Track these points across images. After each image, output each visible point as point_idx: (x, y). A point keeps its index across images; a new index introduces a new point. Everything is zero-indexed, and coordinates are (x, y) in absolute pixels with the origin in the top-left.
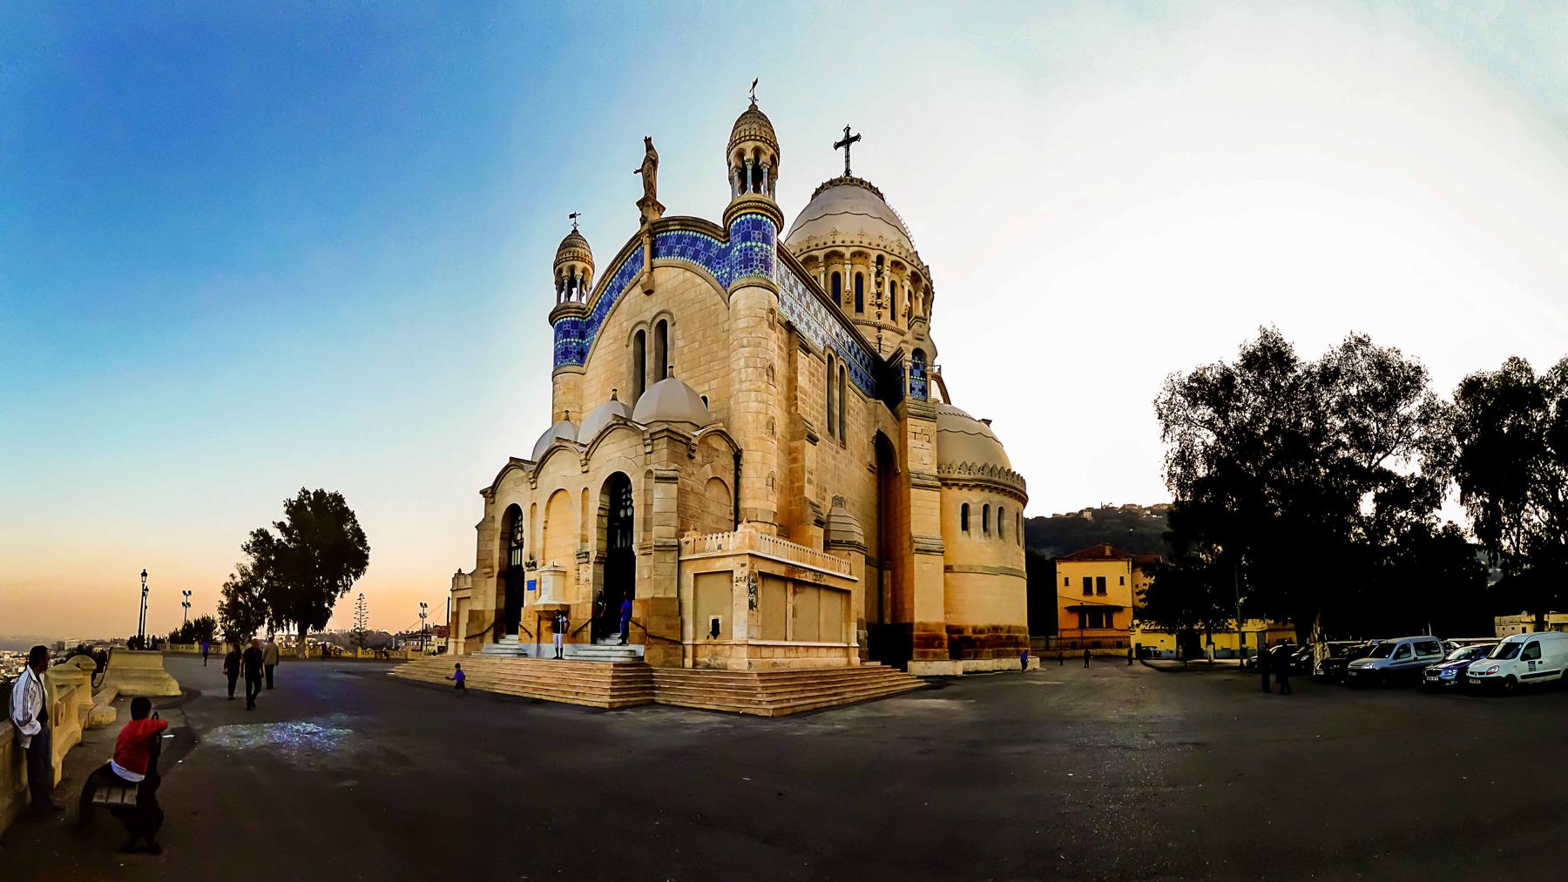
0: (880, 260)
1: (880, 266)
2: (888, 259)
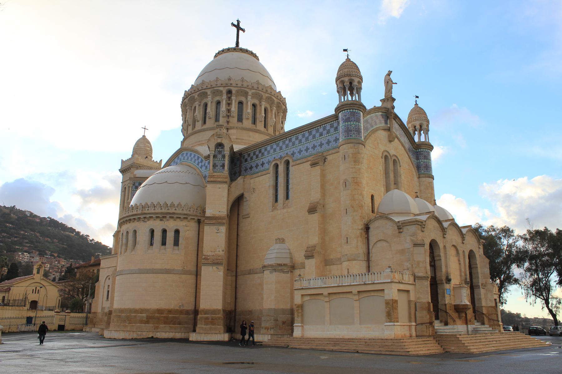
0: (229, 92)
1: (229, 95)
2: (234, 90)
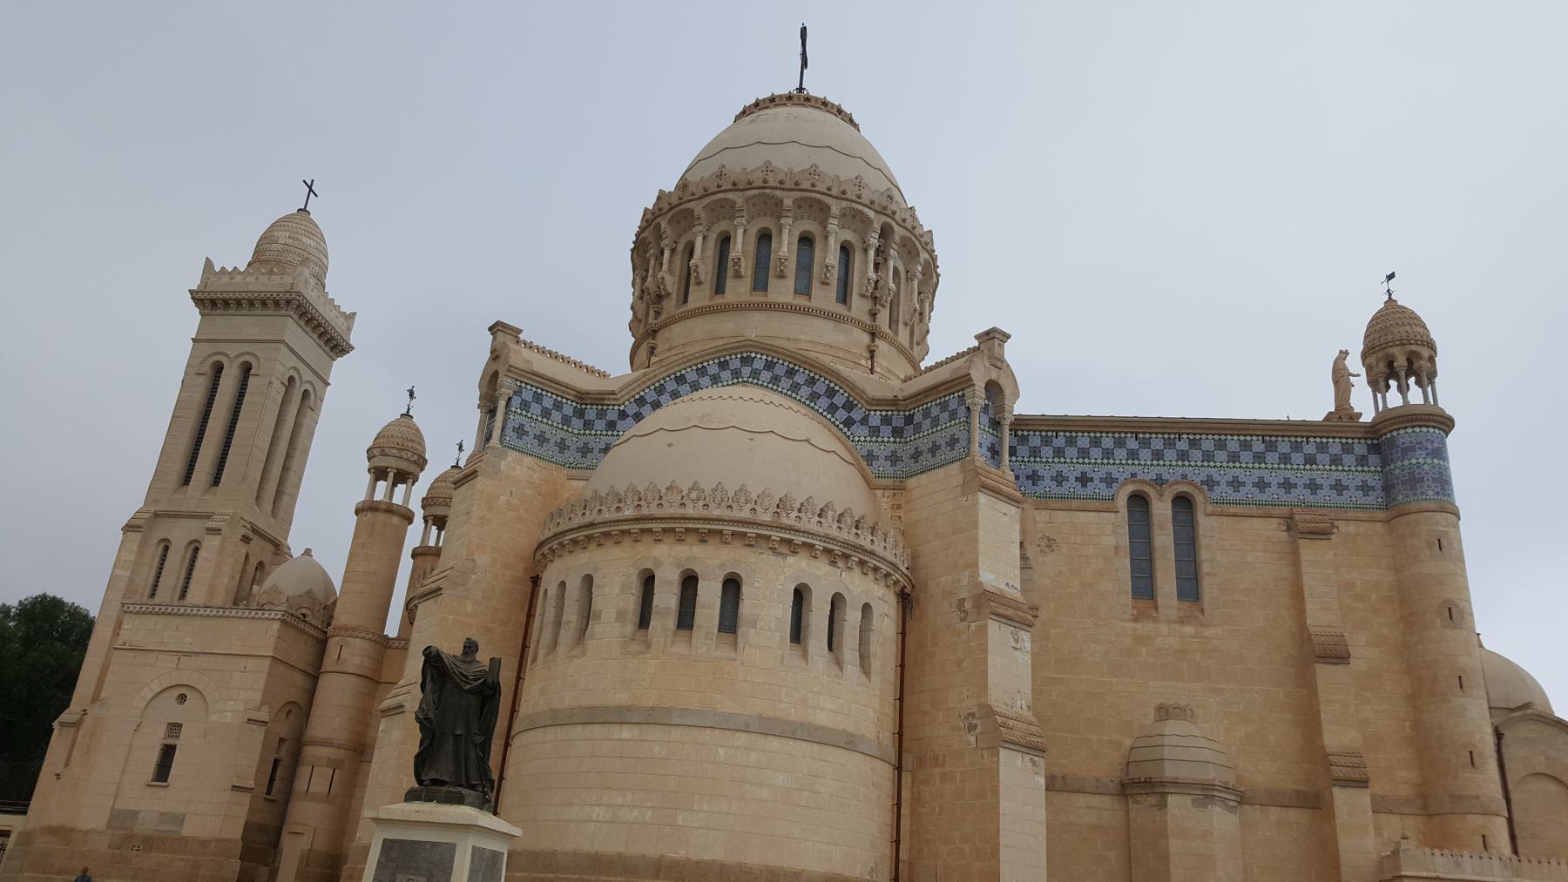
2: (899, 232)
